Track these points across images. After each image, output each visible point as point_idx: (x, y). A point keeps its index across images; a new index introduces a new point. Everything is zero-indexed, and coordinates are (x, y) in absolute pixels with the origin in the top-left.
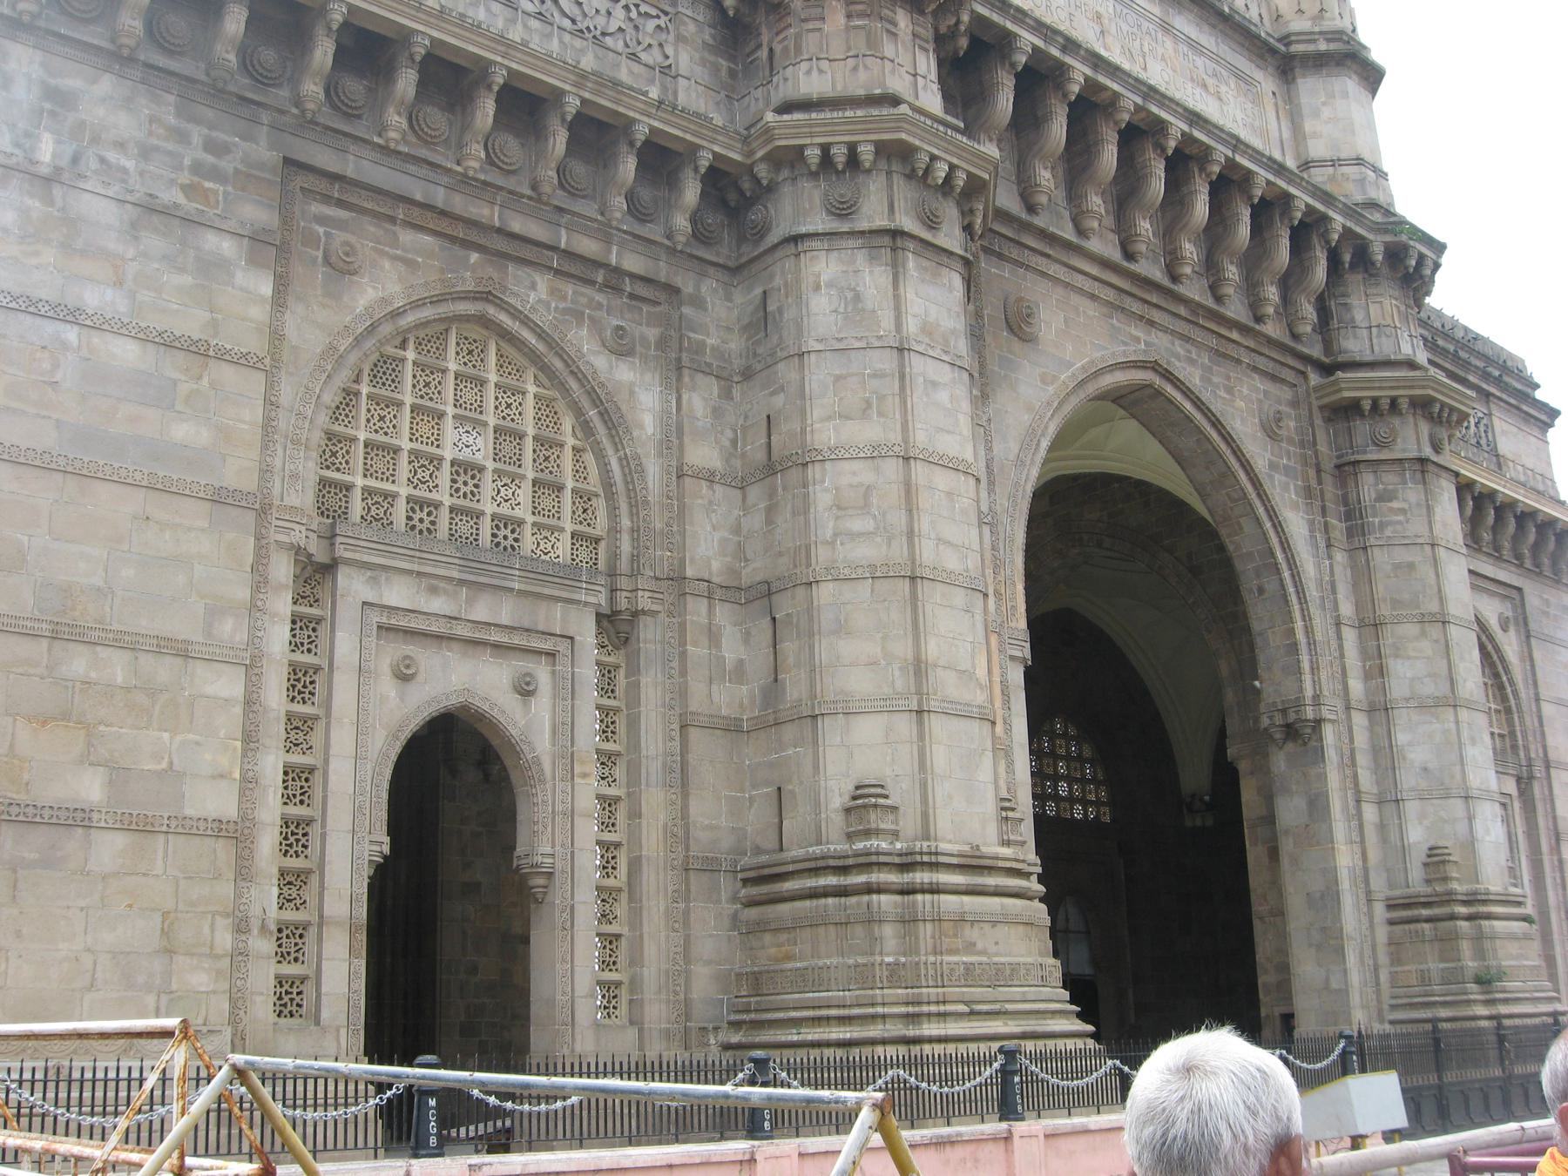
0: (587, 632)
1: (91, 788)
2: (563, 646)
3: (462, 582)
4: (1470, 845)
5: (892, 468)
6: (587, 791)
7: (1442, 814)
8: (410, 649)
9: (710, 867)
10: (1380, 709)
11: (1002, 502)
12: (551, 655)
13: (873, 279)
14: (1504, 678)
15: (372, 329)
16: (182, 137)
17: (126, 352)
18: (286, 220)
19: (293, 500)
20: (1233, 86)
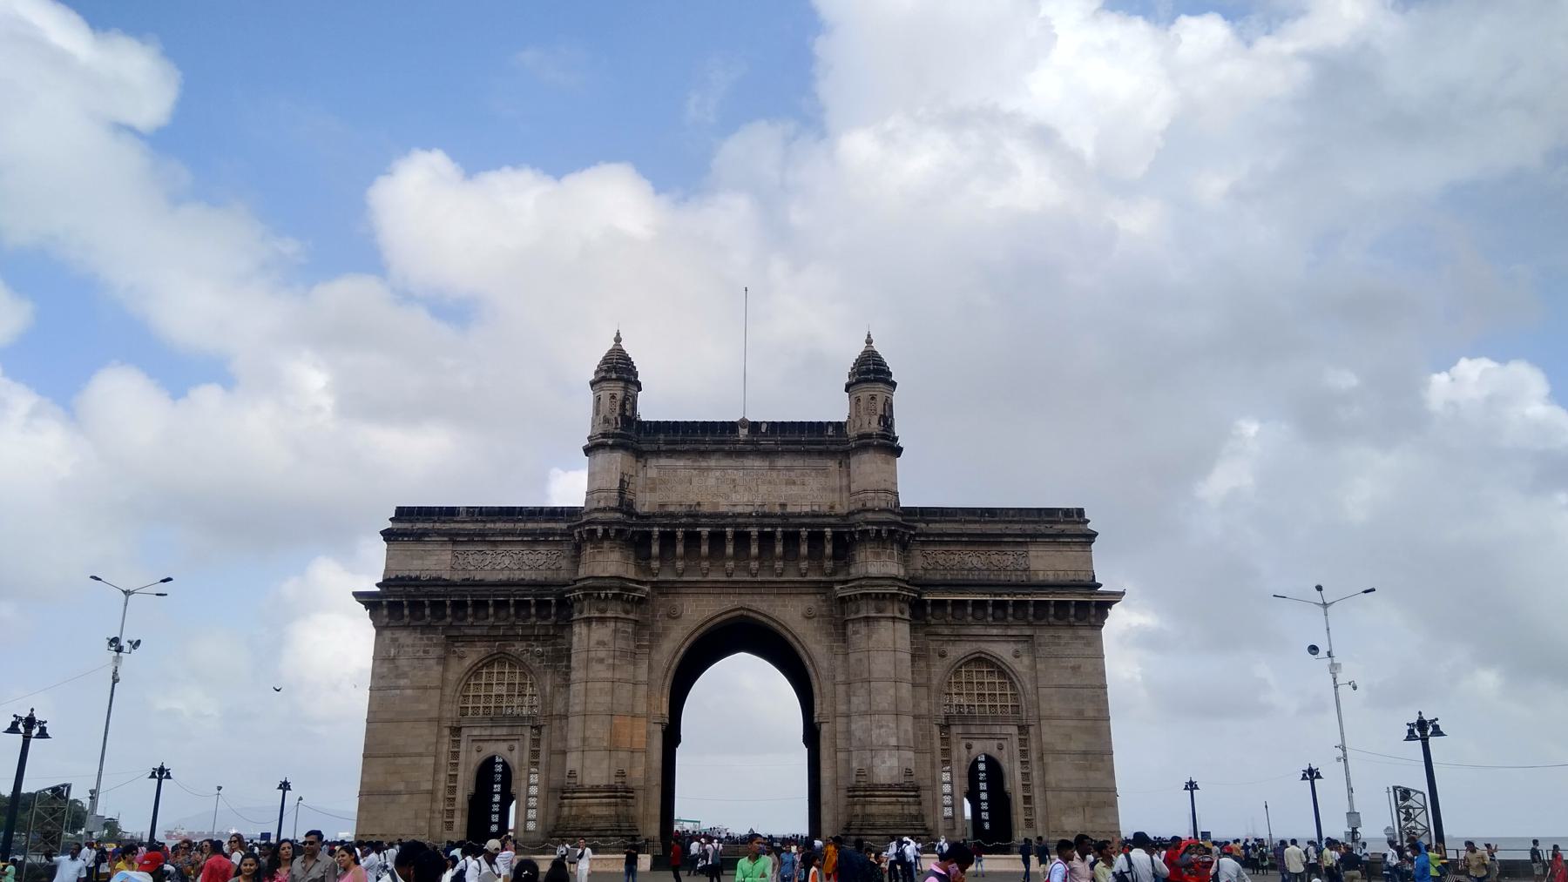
0: (528, 733)
1: (401, 786)
2: (520, 737)
3: (492, 726)
4: (871, 768)
5: (583, 684)
6: (525, 775)
7: (864, 757)
8: (480, 744)
9: (554, 790)
10: (848, 716)
11: (658, 674)
12: (518, 740)
13: (584, 630)
14: (1015, 680)
15: (471, 669)
16: (422, 639)
17: (409, 692)
18: (448, 651)
19: (449, 716)
20: (813, 474)
